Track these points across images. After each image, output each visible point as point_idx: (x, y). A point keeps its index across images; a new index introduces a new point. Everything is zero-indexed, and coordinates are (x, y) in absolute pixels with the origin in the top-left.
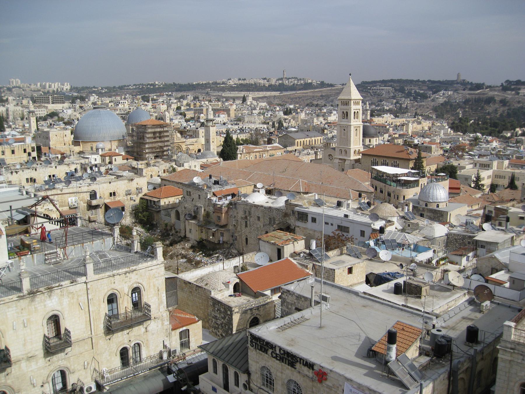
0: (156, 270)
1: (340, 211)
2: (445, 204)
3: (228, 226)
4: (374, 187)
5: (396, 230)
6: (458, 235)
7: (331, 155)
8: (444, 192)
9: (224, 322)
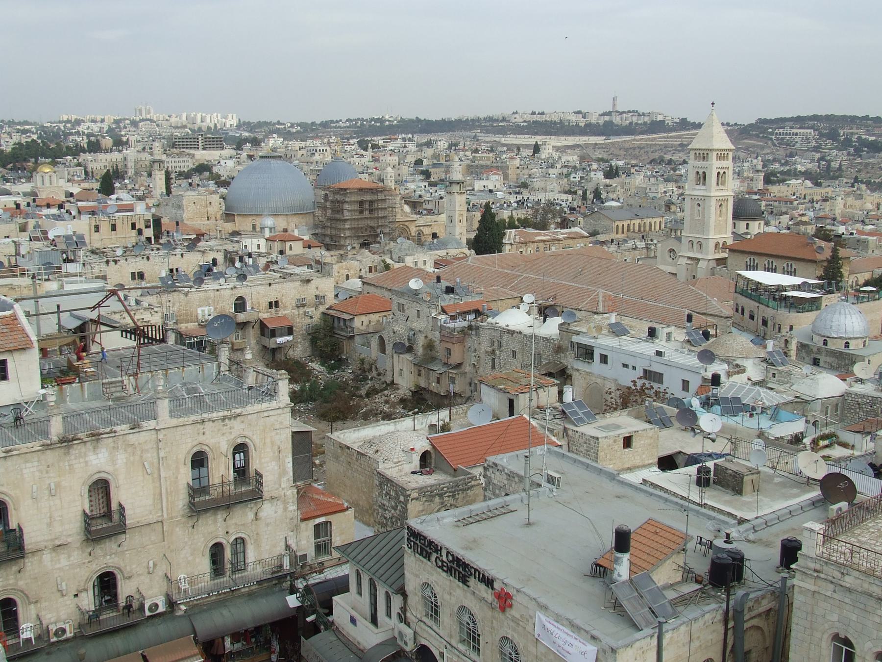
0: (276, 417)
1: (652, 345)
2: (861, 342)
3: (463, 367)
5: (750, 382)
6: (864, 396)
7: (674, 250)
8: (859, 320)
9: (395, 515)
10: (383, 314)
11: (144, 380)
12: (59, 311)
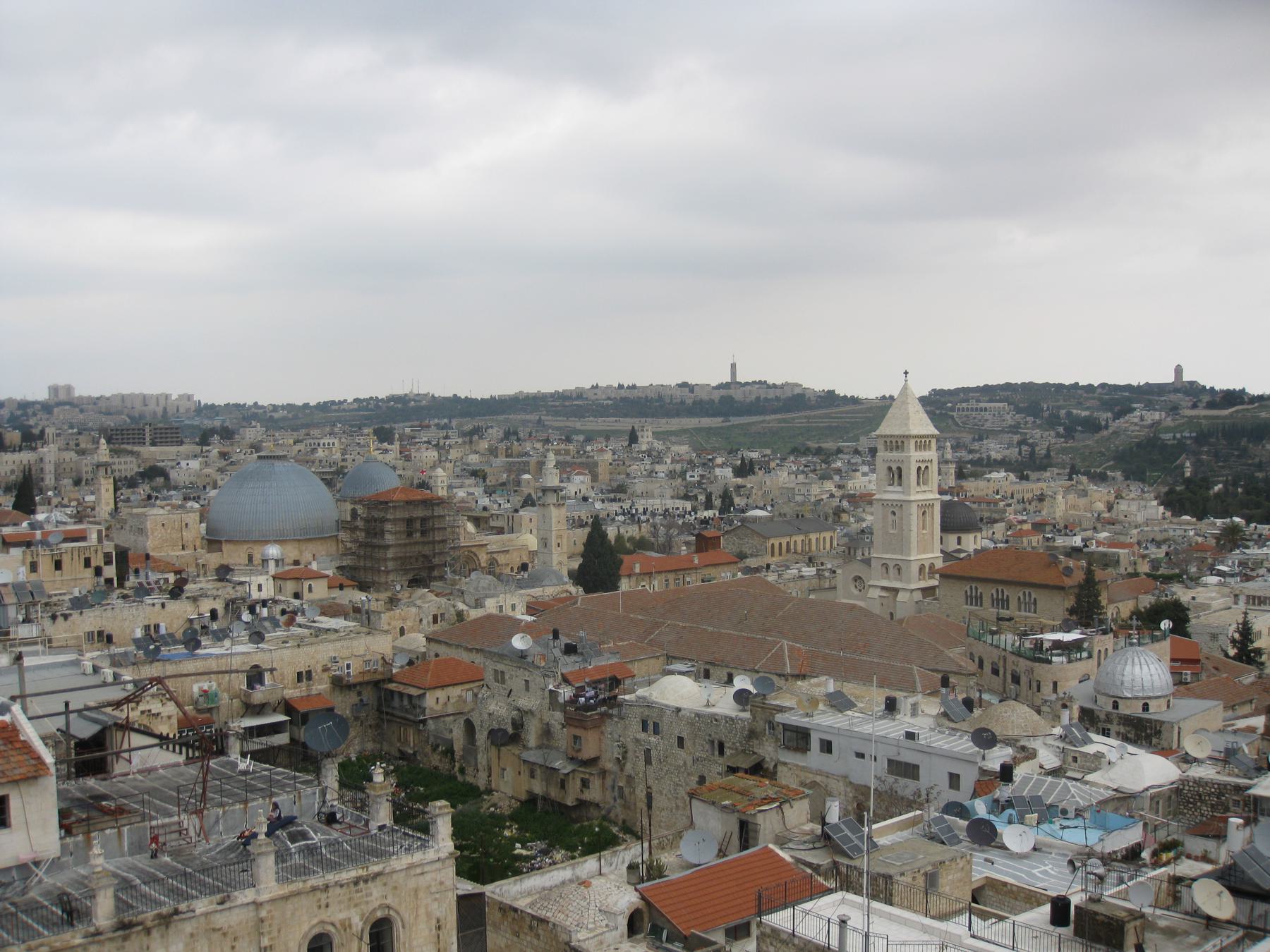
0: (433, 875)
2: (1163, 702)
4: (977, 660)
7: (860, 578)
10: (467, 686)
11: (212, 820)
12: (67, 711)
